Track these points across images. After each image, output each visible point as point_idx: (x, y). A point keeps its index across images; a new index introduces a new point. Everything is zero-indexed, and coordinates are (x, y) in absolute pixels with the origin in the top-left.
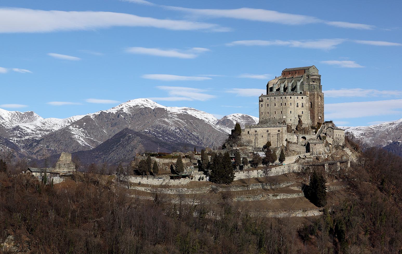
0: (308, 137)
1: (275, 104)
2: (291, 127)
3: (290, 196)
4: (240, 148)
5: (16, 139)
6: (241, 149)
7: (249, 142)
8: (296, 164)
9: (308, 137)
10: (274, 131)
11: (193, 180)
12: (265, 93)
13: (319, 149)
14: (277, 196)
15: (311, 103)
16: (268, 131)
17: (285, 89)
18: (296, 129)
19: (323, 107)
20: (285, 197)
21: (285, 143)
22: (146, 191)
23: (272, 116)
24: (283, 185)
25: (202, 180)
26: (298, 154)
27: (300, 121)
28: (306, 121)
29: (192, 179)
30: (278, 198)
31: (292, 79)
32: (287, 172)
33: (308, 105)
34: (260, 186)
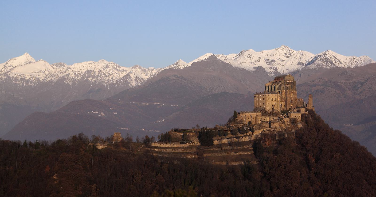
2: (268, 112)
3: (246, 153)
4: (234, 125)
5: (344, 82)
7: (242, 121)
10: (254, 115)
11: (191, 144)
13: (276, 125)
14: (237, 153)
16: (251, 115)
18: (271, 113)
20: (242, 153)
21: (260, 122)
22: (159, 151)
23: (259, 106)
24: (245, 147)
25: (197, 144)
26: (266, 128)
27: (273, 109)
29: (190, 144)
30: (238, 154)
31: (276, 83)
34: (229, 148)
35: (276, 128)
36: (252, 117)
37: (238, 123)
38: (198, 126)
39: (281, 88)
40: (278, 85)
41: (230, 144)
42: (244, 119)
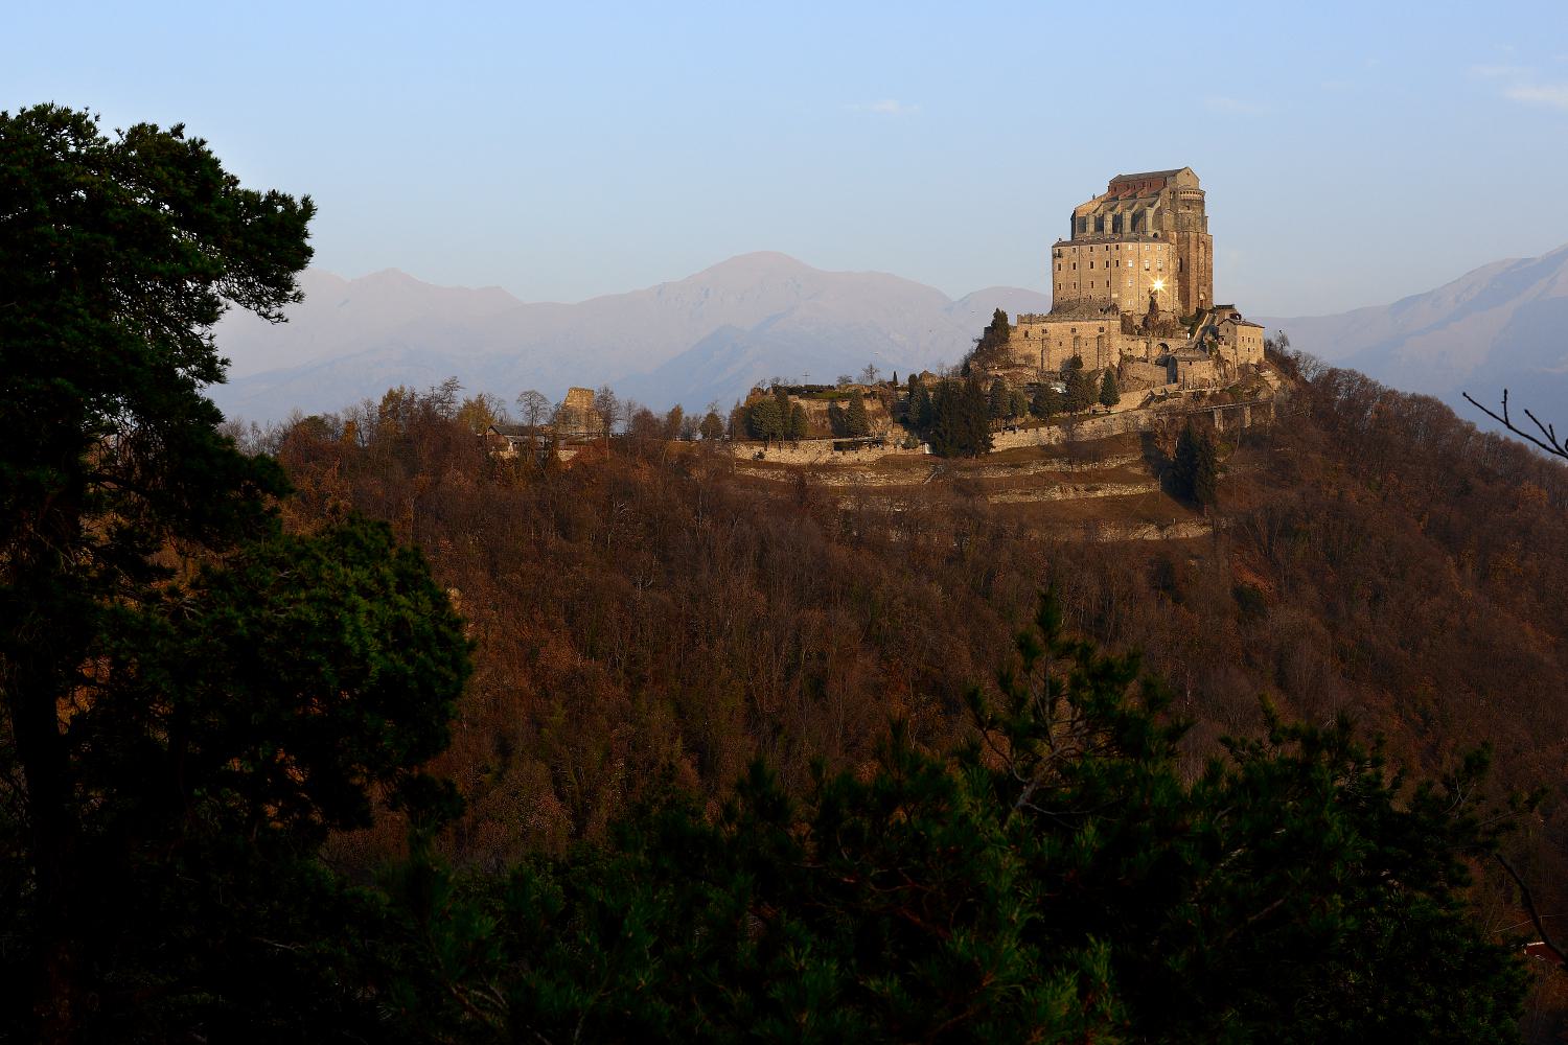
0: (1172, 344)
1: (1092, 263)
2: (1130, 318)
3: (1127, 491)
6: (1008, 375)
7: (1029, 358)
8: (1142, 412)
9: (1172, 344)
10: (1088, 328)
12: (1068, 238)
15: (1181, 259)
16: (1074, 330)
17: (1118, 222)
18: (1144, 324)
19: (1211, 271)
20: (1116, 492)
21: (1116, 359)
26: (1148, 386)
27: (1153, 305)
28: (1169, 305)
30: (1100, 494)
32: (1120, 432)
33: (1173, 266)
34: (1056, 466)
35: (1204, 383)
36: (1076, 338)
37: (1009, 365)
38: (871, 371)
39: (1160, 221)
40: (1153, 210)
41: (1046, 452)
42: (1036, 351)
